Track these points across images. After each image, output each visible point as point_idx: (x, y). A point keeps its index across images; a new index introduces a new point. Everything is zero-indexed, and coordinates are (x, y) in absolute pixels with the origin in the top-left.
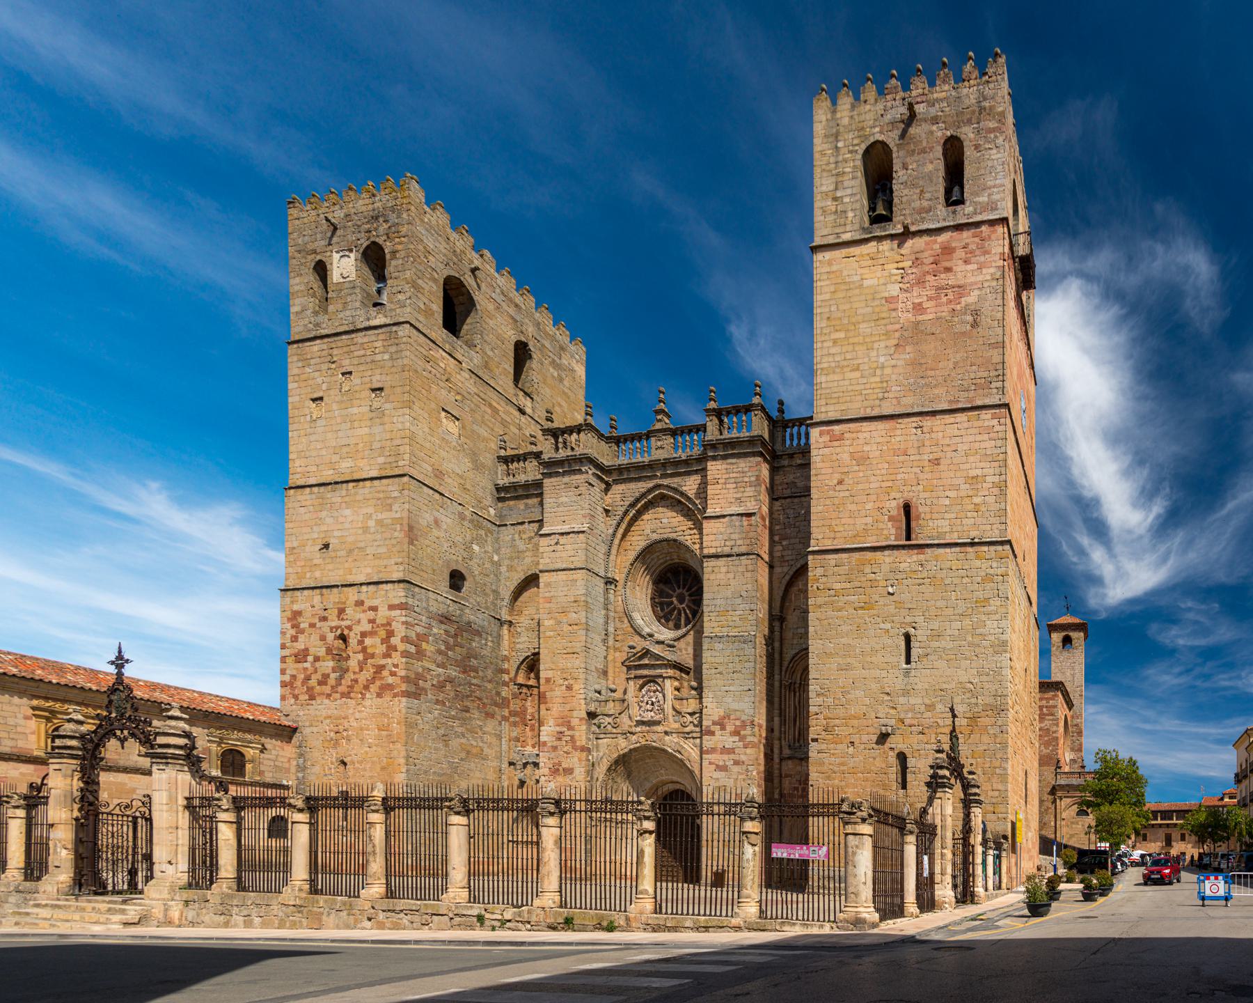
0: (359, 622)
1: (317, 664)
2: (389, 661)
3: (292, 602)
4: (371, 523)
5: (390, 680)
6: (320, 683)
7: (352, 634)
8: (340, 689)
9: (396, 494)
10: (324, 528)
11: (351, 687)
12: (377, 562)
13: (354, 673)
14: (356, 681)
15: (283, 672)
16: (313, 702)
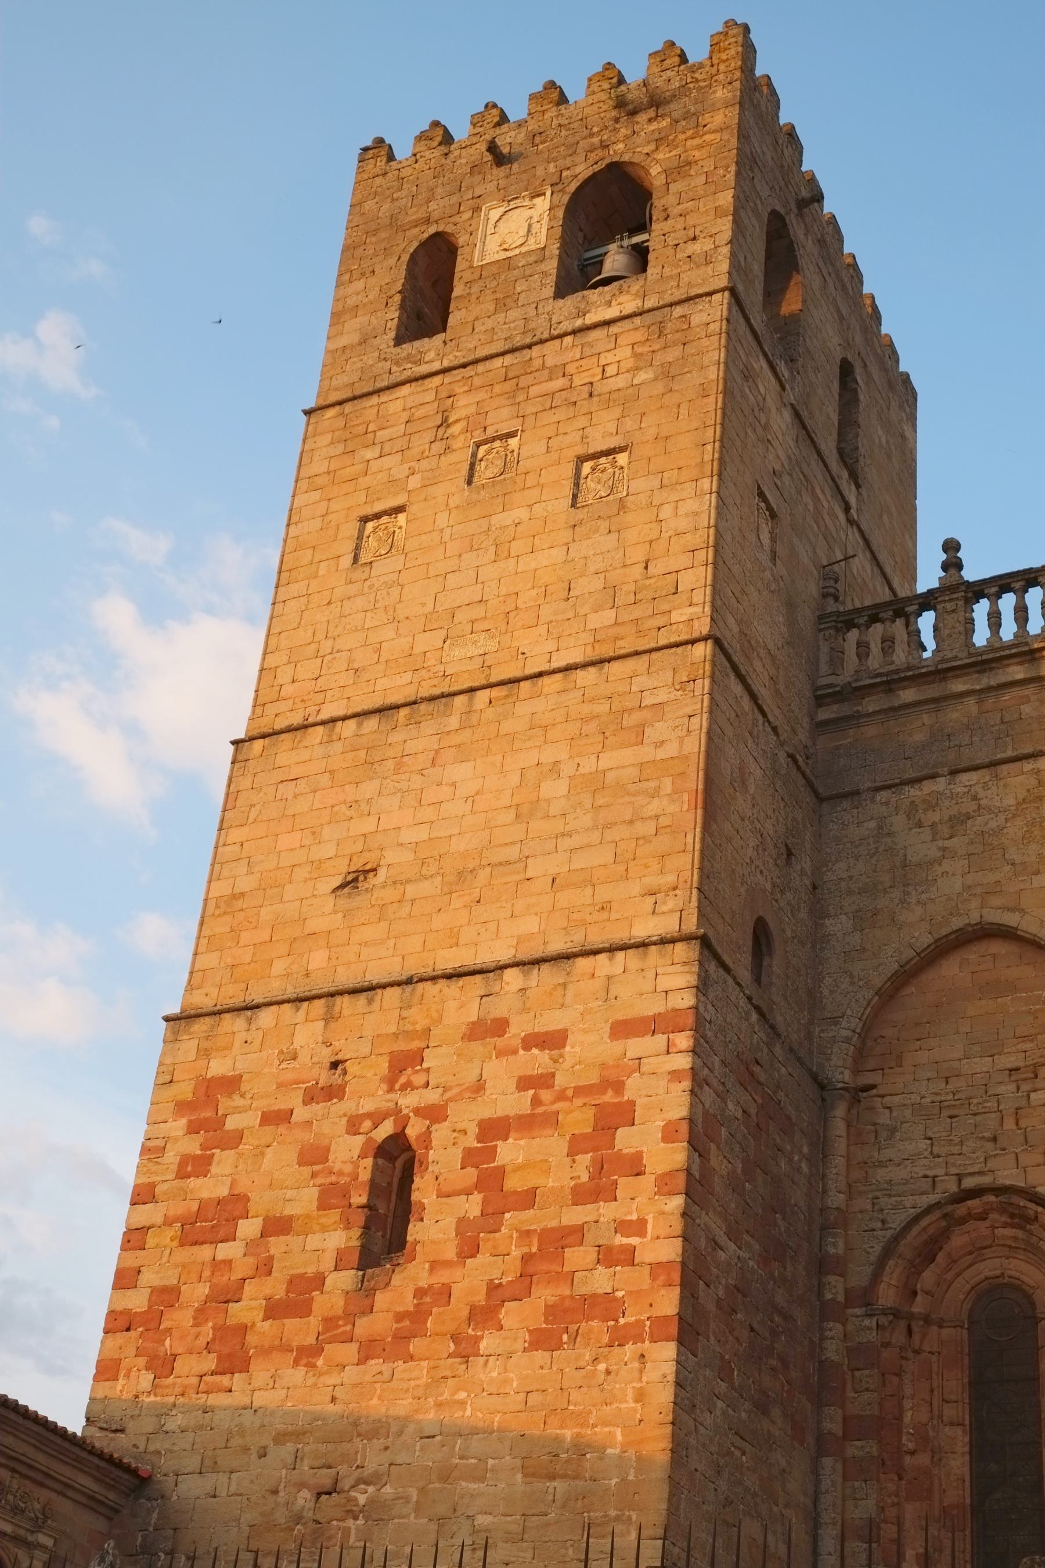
0: (479, 1087)
1: (277, 1245)
2: (607, 1211)
3: (204, 1053)
4: (555, 789)
5: (601, 1281)
6: (274, 1310)
7: (440, 1133)
8: (363, 1326)
9: (662, 696)
10: (368, 825)
11: (418, 1316)
12: (565, 898)
13: (435, 1265)
14: (445, 1293)
15: (125, 1279)
16: (238, 1380)
